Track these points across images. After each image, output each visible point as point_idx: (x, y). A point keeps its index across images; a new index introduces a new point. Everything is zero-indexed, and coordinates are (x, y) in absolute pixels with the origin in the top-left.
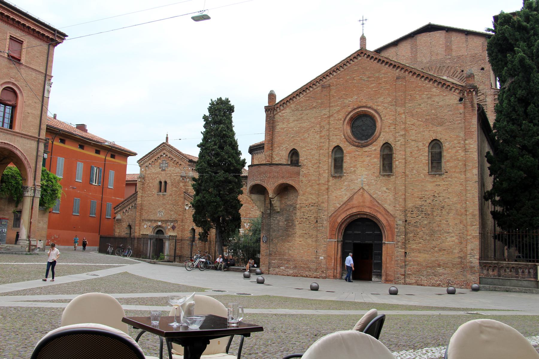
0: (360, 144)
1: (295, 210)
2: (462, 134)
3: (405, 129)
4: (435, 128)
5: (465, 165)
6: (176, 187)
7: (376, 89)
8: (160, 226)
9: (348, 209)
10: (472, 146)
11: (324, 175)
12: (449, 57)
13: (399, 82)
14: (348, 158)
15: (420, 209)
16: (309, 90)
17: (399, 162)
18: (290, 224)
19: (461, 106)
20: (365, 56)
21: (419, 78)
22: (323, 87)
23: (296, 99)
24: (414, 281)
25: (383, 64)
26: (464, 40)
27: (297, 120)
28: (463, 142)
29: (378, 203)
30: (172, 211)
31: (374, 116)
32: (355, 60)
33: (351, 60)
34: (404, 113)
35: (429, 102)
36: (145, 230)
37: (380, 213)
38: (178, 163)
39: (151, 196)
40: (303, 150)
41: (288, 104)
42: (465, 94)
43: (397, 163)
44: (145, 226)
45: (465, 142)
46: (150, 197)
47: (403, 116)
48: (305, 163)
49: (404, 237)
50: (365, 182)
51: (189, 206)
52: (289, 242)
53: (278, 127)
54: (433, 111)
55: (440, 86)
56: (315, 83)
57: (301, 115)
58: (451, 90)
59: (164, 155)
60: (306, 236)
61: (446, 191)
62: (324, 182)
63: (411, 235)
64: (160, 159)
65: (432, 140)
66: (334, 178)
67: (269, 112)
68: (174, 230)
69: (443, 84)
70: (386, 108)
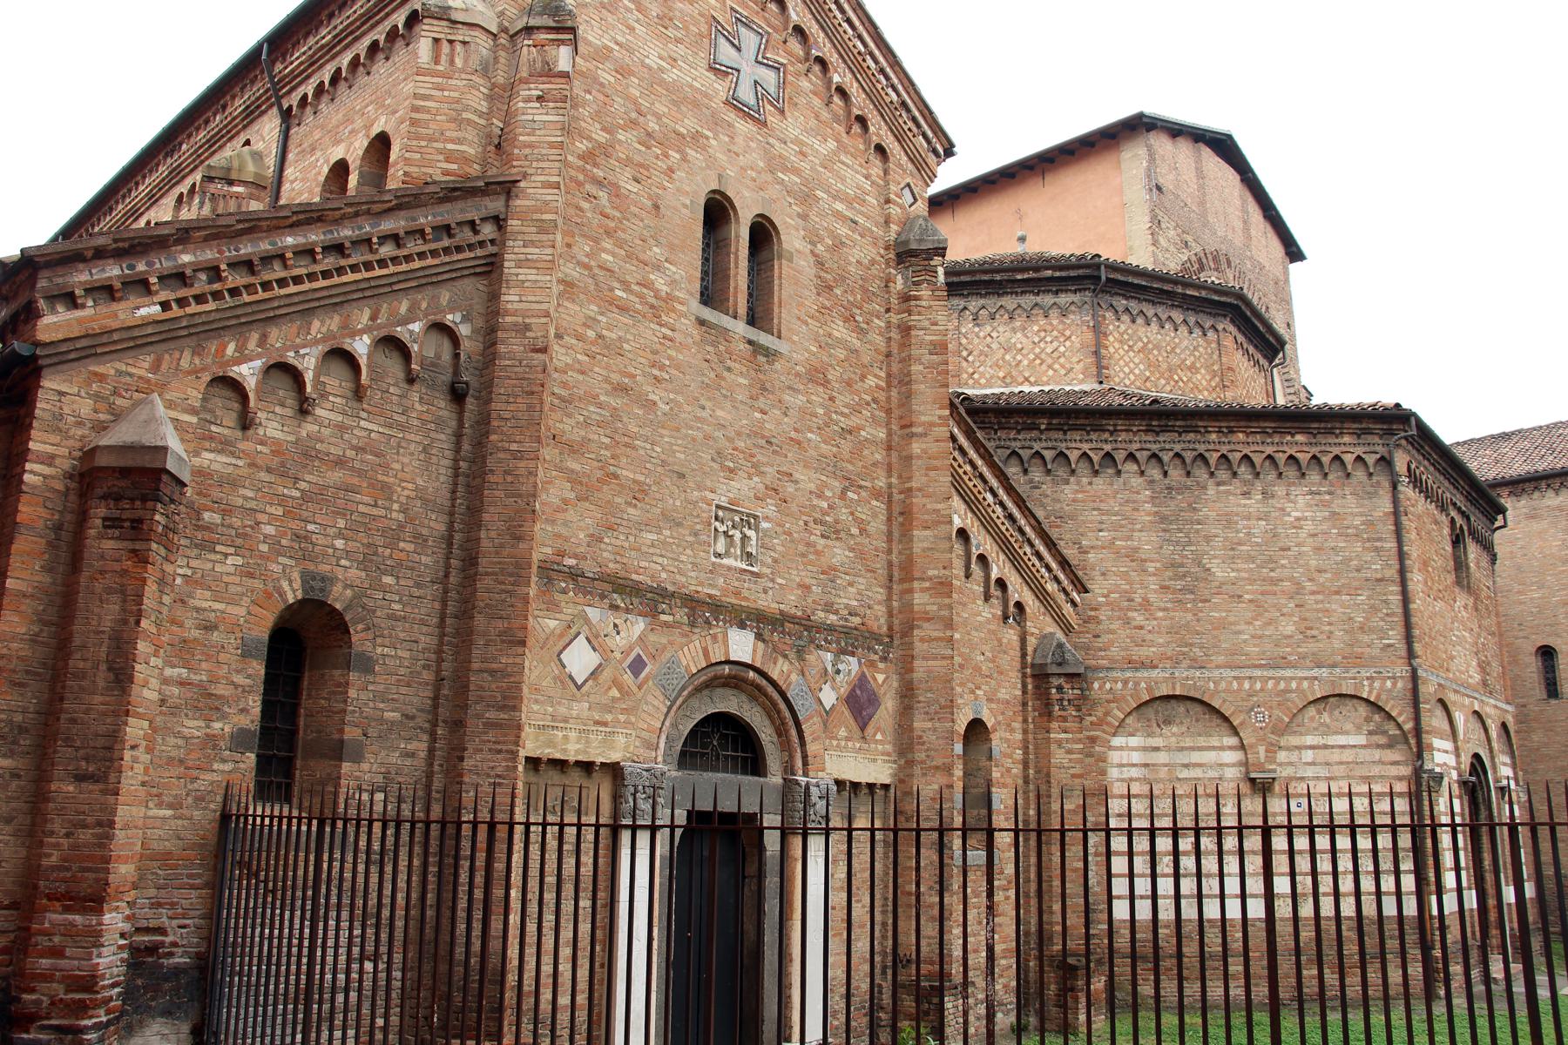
8: (734, 677)
30: (834, 532)
36: (580, 708)
44: (580, 659)
68: (863, 728)
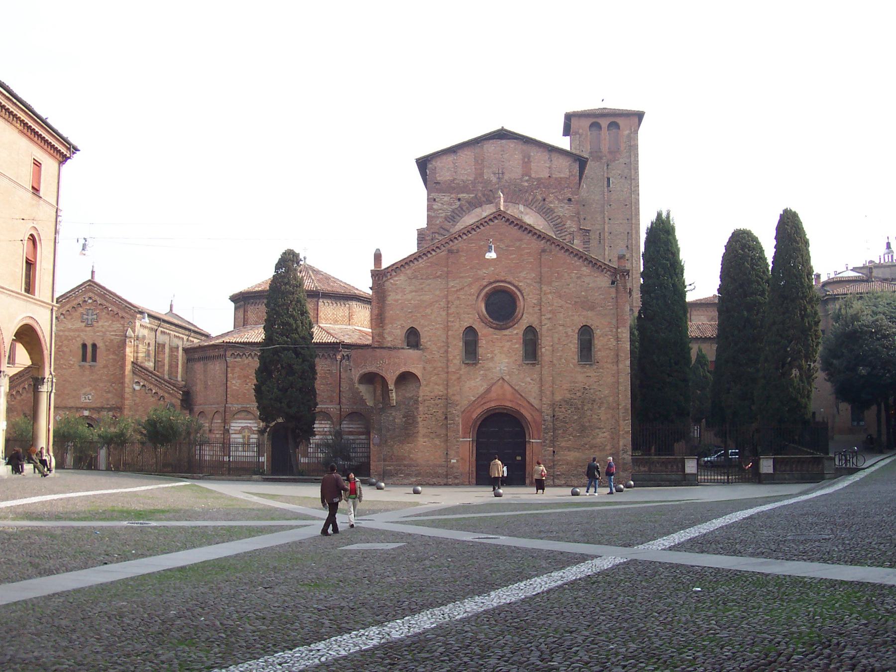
0: (499, 327)
1: (418, 404)
2: (614, 321)
3: (553, 312)
4: (585, 313)
5: (617, 355)
6: (114, 353)
7: (518, 262)
9: (485, 403)
10: (624, 335)
11: (455, 361)
12: (527, 178)
13: (545, 257)
14: (484, 342)
15: (567, 402)
16: (431, 254)
17: (546, 350)
18: (410, 421)
19: (613, 290)
20: (504, 219)
21: (567, 254)
22: (450, 251)
23: (414, 263)
24: (563, 482)
25: (526, 232)
26: (547, 157)
27: (416, 292)
28: (615, 330)
29: (521, 396)
30: (109, 392)
31: (515, 293)
32: (491, 223)
33: (486, 222)
34: (550, 293)
35: (579, 282)
37: (523, 407)
38: (117, 314)
39: (67, 367)
40: (425, 329)
41: (403, 269)
42: (618, 278)
43: (543, 350)
45: (617, 330)
46: (65, 369)
47: (550, 296)
48: (428, 347)
49: (552, 434)
50: (505, 372)
51: (142, 384)
52: (408, 443)
53: (389, 298)
54: (583, 293)
55: (591, 265)
56: (439, 246)
57: (421, 284)
58: (602, 271)
59: (90, 301)
60: (431, 435)
61: (598, 383)
62: (454, 370)
63: (560, 432)
64: (81, 307)
65: (582, 325)
66: (466, 366)
67: (377, 278)
69: (595, 264)
70: (529, 285)
